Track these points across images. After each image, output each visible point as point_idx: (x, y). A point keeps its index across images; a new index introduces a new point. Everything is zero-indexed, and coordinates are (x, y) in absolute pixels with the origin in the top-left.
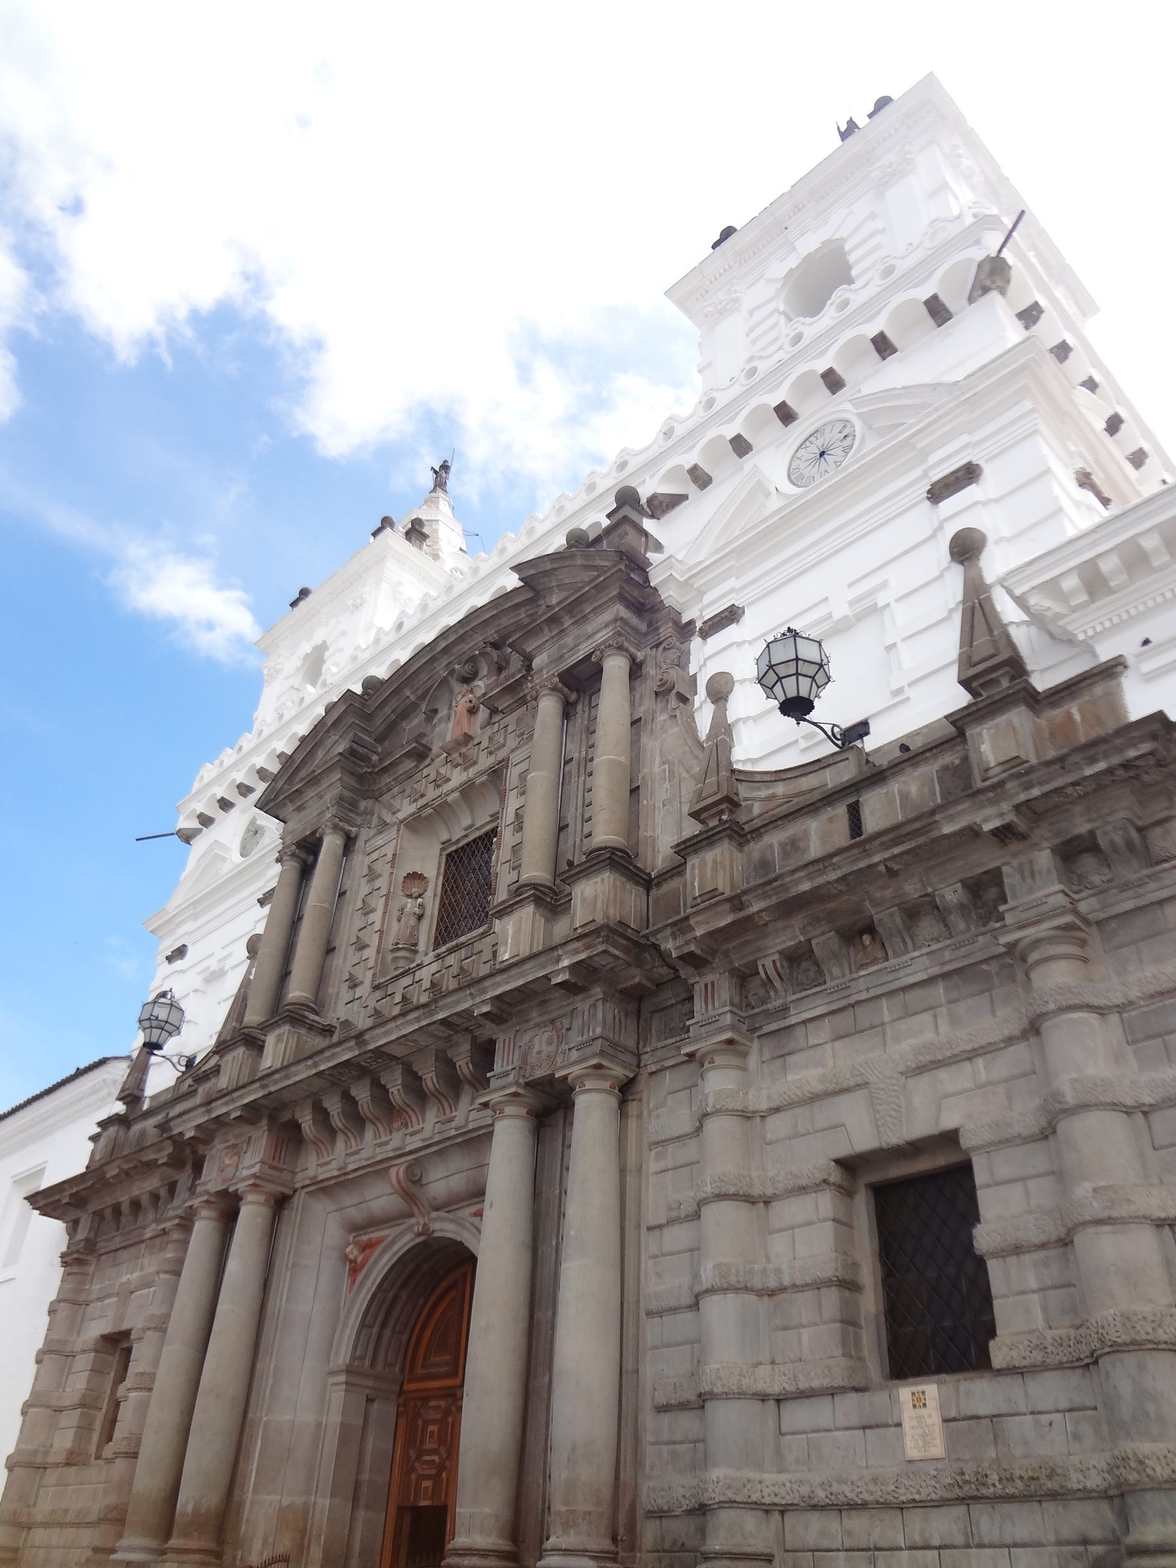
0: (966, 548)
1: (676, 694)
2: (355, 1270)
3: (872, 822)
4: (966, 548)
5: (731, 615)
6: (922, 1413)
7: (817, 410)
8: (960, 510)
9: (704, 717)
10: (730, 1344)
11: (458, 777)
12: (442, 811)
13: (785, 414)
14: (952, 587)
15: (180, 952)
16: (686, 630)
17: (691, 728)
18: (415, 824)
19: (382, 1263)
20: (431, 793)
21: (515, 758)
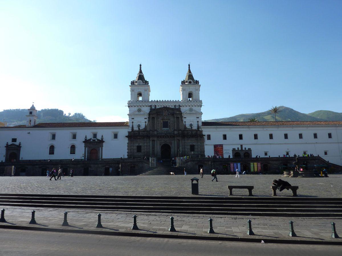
0: (198, 122)
1: (182, 120)
2: (160, 144)
3: (193, 133)
4: (198, 122)
5: (186, 118)
6: (192, 153)
7: (191, 106)
8: (198, 120)
9: (184, 124)
10: (186, 149)
11: (166, 118)
12: (164, 119)
13: (189, 106)
14: (197, 123)
15: (133, 119)
16: (183, 117)
17: (183, 124)
18: (162, 119)
19: (162, 145)
20: (163, 118)
21: (171, 119)
